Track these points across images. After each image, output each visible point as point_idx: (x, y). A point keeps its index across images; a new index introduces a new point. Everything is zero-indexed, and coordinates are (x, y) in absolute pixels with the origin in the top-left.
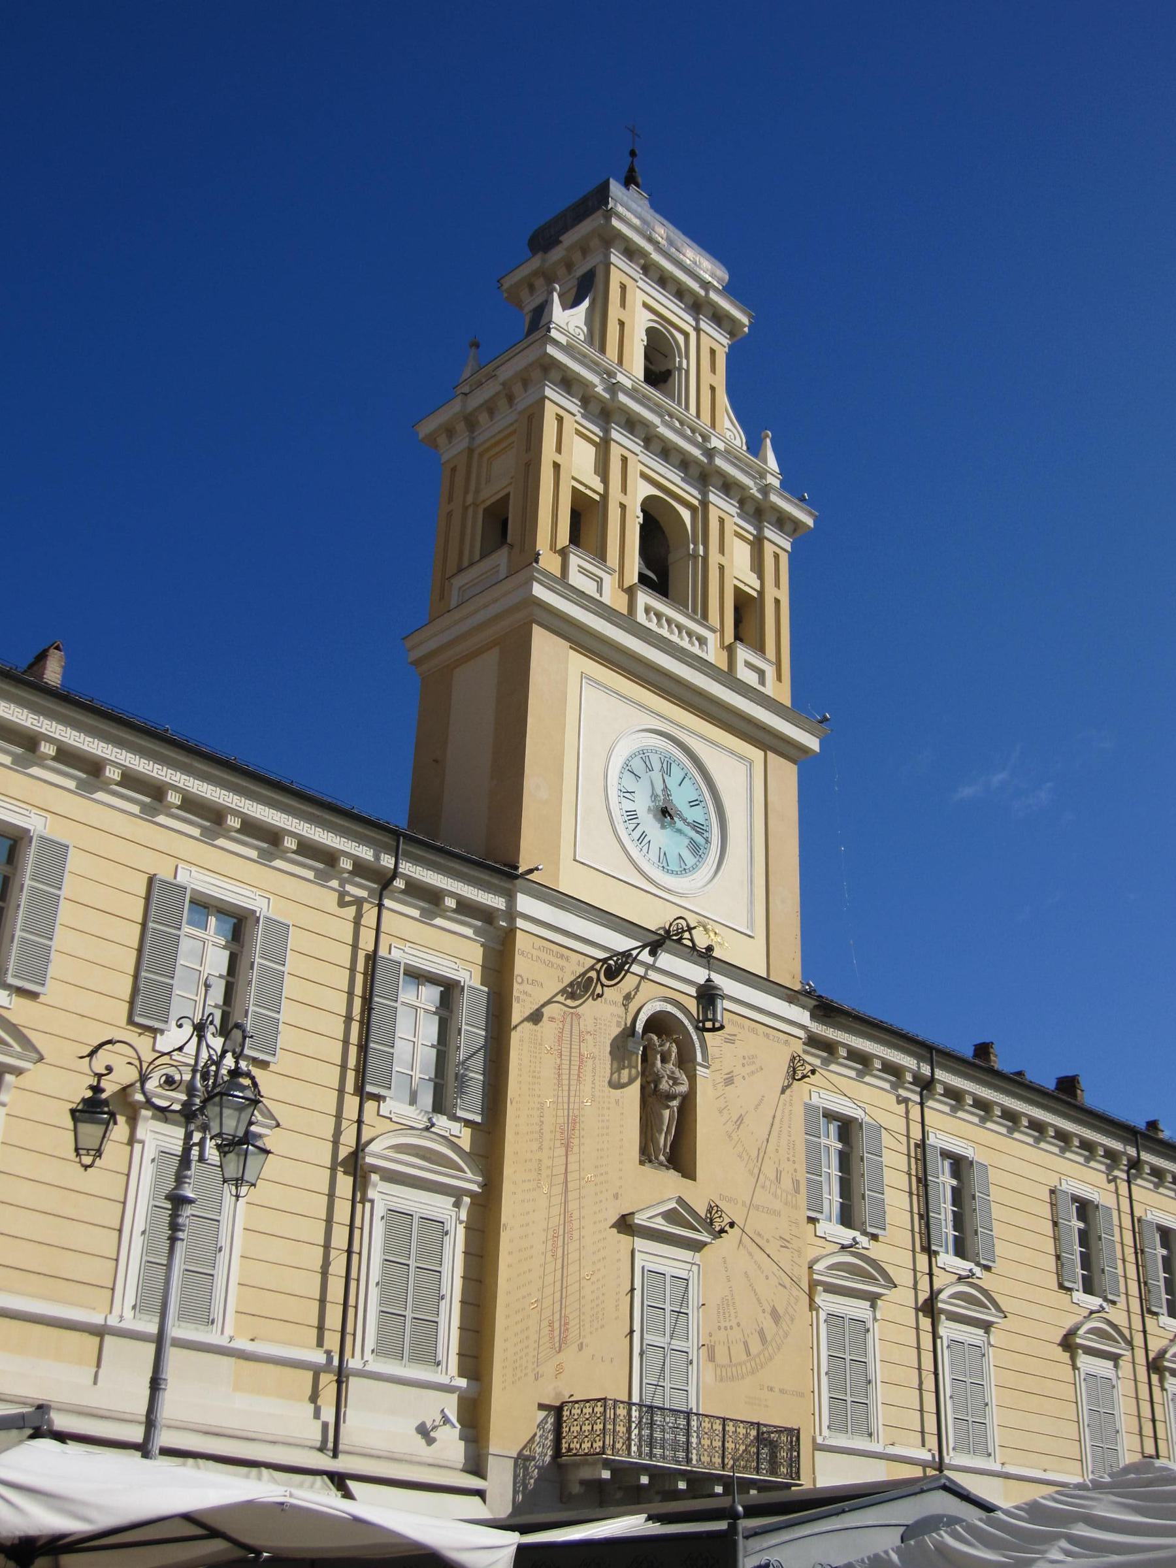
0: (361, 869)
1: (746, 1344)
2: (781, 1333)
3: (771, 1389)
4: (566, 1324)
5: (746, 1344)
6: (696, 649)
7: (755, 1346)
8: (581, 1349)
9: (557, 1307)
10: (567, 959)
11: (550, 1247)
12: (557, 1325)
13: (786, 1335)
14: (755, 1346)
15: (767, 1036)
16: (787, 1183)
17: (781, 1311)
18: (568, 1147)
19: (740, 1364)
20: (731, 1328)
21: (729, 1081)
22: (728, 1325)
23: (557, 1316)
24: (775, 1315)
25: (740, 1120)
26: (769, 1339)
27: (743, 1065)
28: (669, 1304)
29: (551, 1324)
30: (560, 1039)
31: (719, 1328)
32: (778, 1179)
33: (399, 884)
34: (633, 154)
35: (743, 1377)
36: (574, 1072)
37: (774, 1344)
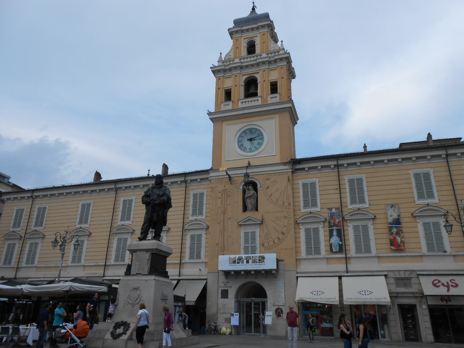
0: (181, 182)
1: (274, 242)
2: (285, 237)
3: (282, 249)
4: (225, 246)
5: (274, 242)
6: (256, 103)
7: (276, 241)
8: (228, 250)
9: (222, 244)
10: (223, 180)
11: (220, 234)
12: (222, 247)
13: (287, 237)
14: (276, 241)
15: (280, 175)
16: (286, 204)
17: (284, 232)
18: (224, 214)
19: (272, 246)
20: (269, 239)
21: (268, 188)
22: (268, 238)
23: (222, 245)
24: (283, 233)
25: (271, 195)
26: (281, 239)
27: (272, 183)
29: (221, 247)
30: (222, 195)
31: (265, 239)
32: (283, 204)
33: (189, 181)
34: (253, 3)
35: (273, 248)
36: (226, 200)
37: (283, 240)
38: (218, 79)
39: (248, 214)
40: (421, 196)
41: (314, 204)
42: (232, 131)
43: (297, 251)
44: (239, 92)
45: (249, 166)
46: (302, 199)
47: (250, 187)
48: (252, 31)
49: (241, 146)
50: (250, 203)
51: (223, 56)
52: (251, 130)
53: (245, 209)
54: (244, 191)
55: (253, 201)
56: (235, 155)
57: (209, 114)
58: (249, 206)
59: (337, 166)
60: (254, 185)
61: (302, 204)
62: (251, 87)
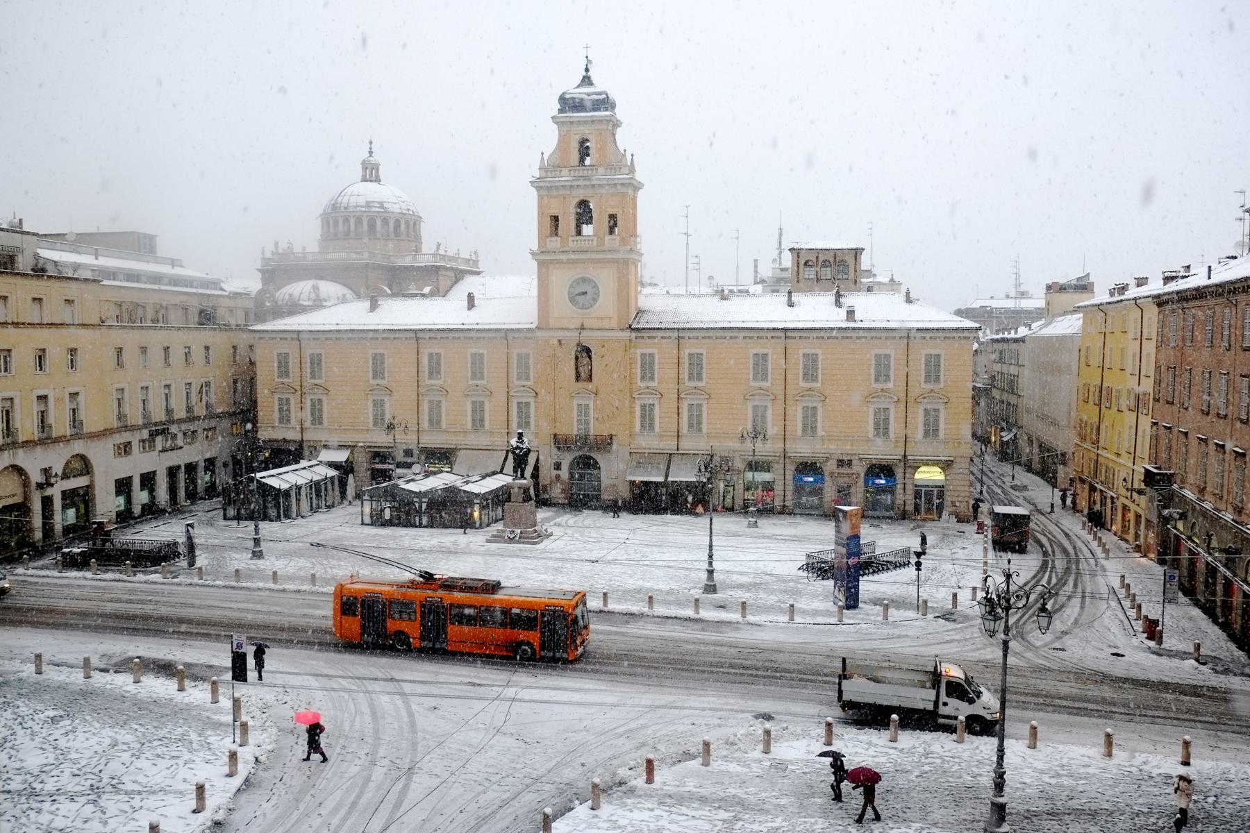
28: (583, 410)
38: (541, 198)
39: (580, 384)
40: (755, 379)
41: (652, 378)
42: (562, 280)
43: (632, 426)
44: (568, 223)
45: (582, 328)
46: (639, 370)
47: (584, 354)
48: (586, 118)
49: (572, 300)
50: (584, 372)
51: (546, 158)
52: (584, 280)
53: (578, 378)
54: (577, 358)
55: (587, 368)
56: (565, 312)
57: (533, 254)
58: (583, 375)
59: (679, 338)
60: (588, 351)
61: (639, 375)
62: (584, 213)
